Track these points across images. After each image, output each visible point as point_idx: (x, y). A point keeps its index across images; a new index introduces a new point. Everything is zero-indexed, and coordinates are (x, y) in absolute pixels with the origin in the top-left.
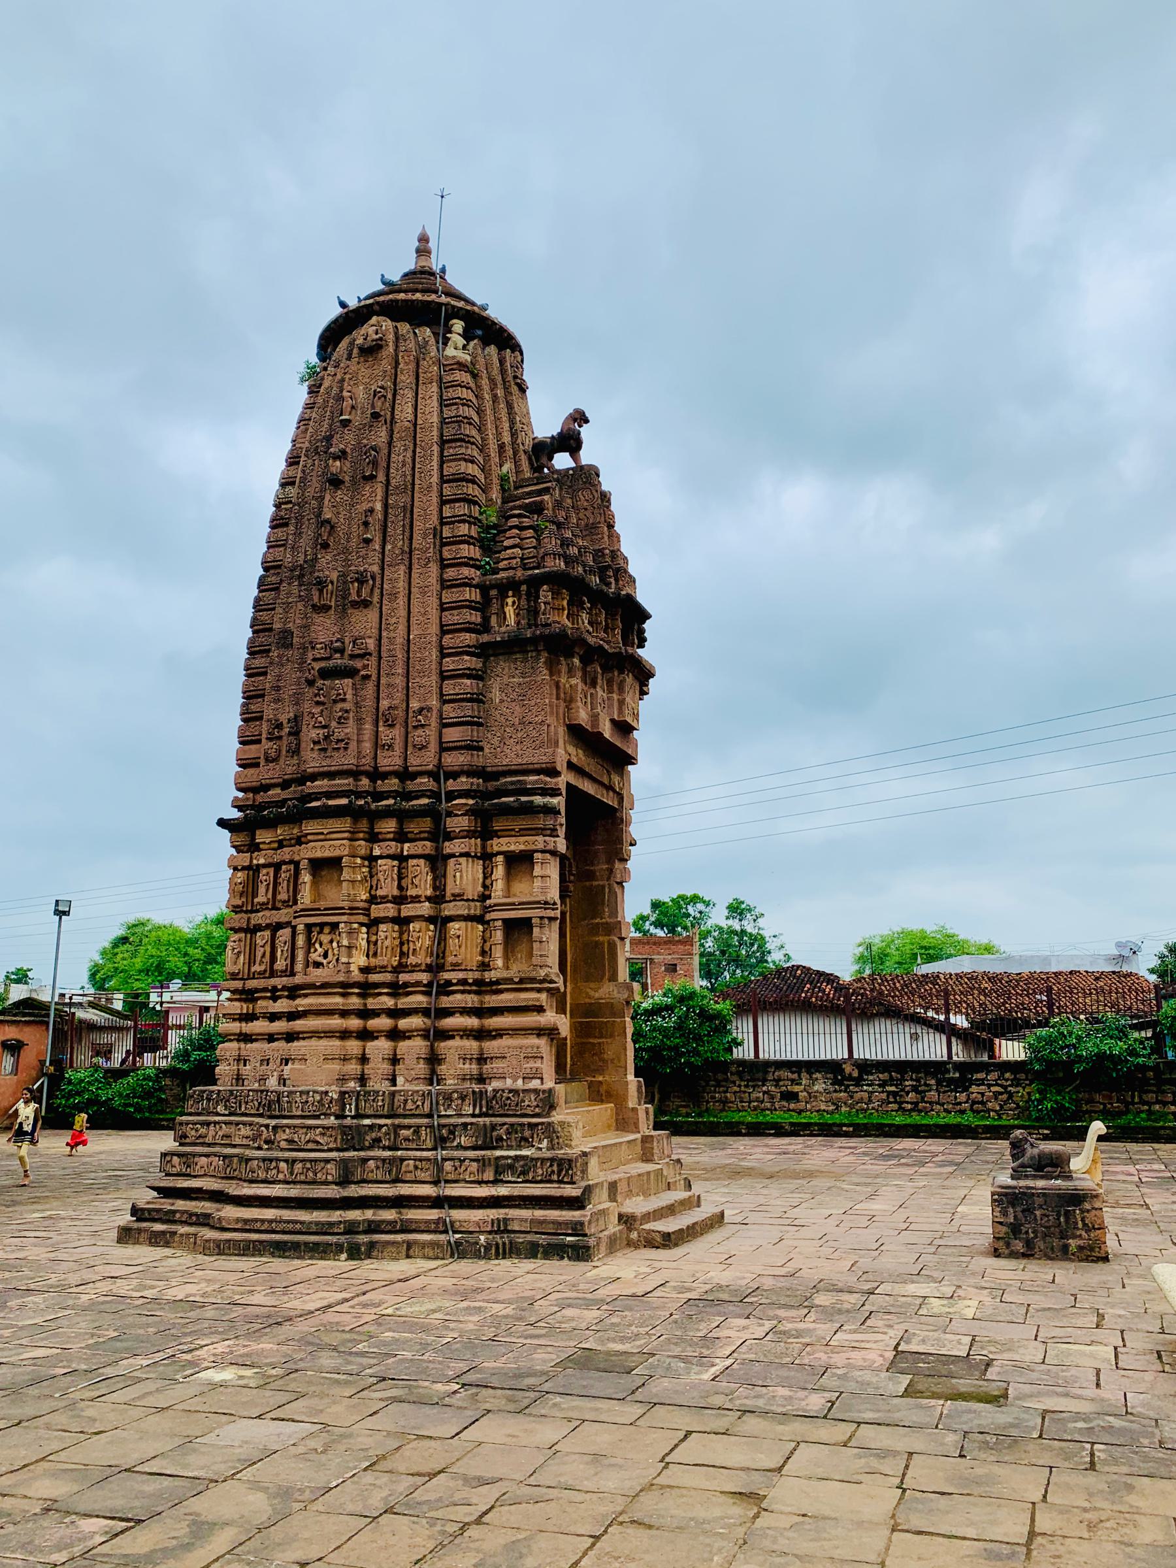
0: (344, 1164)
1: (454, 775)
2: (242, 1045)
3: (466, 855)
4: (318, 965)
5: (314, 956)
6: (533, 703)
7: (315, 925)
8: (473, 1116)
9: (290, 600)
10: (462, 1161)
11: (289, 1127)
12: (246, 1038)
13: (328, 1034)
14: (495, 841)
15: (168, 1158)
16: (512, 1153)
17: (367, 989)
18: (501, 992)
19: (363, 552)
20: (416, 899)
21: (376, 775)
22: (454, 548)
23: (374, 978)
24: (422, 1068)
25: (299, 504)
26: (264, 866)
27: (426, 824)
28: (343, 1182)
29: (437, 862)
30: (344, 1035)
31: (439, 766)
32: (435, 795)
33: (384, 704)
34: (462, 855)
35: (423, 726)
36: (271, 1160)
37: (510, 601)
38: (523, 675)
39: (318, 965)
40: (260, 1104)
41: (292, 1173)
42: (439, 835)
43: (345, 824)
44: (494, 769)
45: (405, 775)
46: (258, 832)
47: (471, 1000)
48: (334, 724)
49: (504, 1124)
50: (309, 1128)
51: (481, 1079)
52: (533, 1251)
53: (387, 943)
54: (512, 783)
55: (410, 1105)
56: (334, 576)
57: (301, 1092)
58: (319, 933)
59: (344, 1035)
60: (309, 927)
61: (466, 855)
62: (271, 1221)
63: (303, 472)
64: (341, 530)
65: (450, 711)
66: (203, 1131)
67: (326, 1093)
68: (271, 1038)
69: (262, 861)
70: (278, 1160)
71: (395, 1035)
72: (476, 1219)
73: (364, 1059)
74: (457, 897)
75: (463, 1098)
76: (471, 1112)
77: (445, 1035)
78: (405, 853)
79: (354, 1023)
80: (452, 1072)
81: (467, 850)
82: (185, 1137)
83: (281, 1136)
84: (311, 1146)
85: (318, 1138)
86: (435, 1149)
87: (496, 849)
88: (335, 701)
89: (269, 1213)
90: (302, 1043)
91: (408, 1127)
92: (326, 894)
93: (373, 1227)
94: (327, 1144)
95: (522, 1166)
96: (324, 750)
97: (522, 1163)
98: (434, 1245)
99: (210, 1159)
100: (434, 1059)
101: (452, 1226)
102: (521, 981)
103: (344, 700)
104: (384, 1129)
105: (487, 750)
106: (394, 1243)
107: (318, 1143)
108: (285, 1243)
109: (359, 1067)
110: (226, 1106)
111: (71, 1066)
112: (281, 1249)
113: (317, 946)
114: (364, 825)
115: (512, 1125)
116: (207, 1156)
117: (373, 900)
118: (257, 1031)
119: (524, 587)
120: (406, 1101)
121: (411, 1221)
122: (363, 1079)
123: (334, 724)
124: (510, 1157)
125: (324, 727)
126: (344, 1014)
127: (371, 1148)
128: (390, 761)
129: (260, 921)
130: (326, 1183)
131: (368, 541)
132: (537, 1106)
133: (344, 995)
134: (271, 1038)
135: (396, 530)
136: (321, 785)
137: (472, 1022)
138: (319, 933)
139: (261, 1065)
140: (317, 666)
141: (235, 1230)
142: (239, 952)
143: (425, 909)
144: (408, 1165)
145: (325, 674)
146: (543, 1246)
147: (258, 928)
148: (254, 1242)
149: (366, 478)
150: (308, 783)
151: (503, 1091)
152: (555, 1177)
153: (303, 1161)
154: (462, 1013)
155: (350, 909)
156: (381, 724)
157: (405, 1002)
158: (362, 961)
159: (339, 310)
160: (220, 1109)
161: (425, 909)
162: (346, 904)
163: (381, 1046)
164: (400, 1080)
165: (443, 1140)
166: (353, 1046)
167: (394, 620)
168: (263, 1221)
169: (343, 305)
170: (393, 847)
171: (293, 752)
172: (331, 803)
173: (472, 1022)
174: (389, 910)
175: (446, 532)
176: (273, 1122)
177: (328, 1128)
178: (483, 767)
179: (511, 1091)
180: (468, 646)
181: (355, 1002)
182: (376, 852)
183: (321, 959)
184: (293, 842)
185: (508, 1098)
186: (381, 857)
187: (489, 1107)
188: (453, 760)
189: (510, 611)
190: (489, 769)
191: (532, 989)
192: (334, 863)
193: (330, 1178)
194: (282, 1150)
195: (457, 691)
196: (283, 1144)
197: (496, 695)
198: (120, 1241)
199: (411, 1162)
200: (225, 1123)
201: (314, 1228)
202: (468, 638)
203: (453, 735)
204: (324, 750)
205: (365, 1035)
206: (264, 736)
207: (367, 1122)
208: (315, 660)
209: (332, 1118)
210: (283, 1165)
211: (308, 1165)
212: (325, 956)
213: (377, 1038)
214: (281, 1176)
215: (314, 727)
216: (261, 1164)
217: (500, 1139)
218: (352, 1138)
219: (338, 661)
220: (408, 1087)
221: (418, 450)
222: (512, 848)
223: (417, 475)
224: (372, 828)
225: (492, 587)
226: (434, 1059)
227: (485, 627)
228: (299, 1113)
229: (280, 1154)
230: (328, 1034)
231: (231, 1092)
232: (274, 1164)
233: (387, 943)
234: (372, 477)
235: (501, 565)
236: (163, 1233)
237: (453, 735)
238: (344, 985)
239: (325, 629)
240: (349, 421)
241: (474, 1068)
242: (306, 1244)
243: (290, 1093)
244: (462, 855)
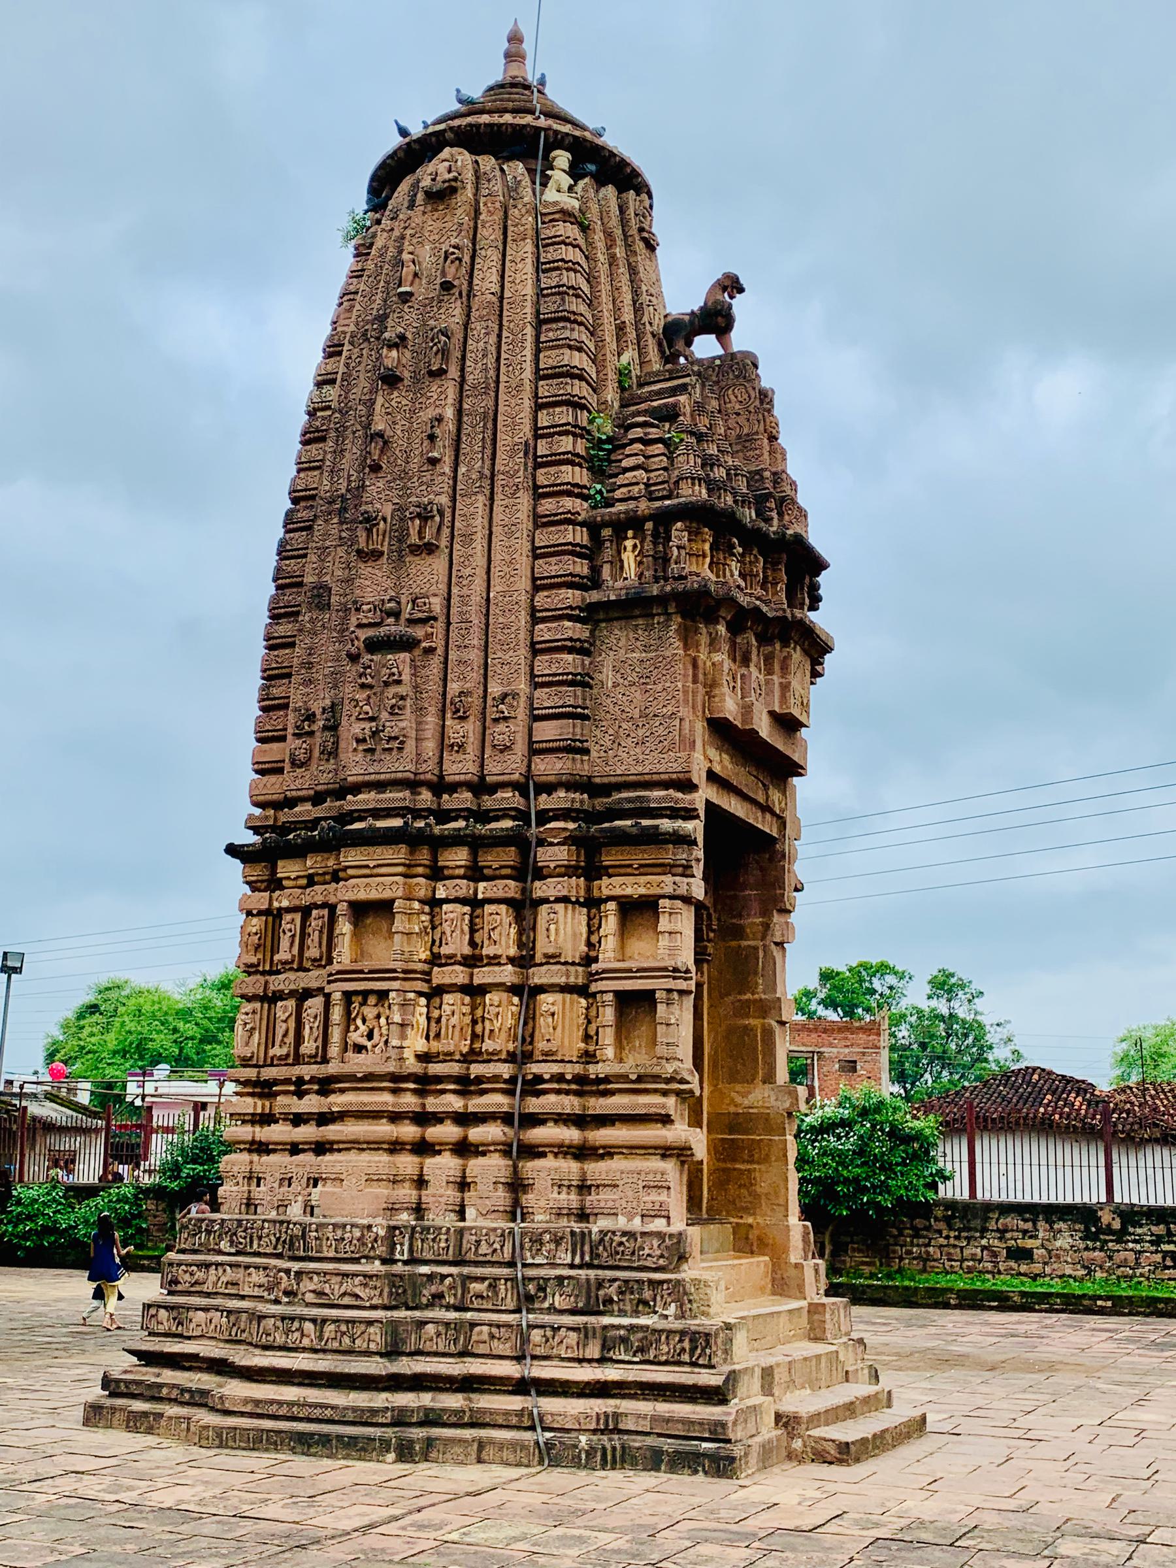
0: (393, 1327)
1: (548, 788)
2: (255, 1157)
3: (564, 900)
4: (359, 1049)
5: (355, 1037)
6: (659, 687)
7: (356, 993)
8: (572, 1266)
9: (328, 543)
10: (555, 1330)
11: (318, 1274)
12: (261, 1148)
13: (373, 1145)
14: (605, 881)
15: (153, 1311)
16: (626, 1321)
17: (426, 1084)
18: (612, 1093)
19: (427, 477)
20: (494, 960)
21: (440, 787)
22: (552, 470)
23: (435, 1069)
24: (501, 1197)
25: (340, 411)
26: (288, 910)
27: (509, 856)
28: (392, 1352)
29: (524, 909)
30: (395, 1147)
31: (528, 775)
32: (522, 816)
33: (454, 687)
34: (558, 900)
35: (506, 719)
36: (292, 1319)
37: (629, 544)
38: (646, 648)
39: (359, 1049)
40: (278, 1239)
41: (321, 1338)
42: (528, 871)
43: (397, 854)
44: (606, 780)
45: (481, 787)
46: (280, 863)
47: (570, 1104)
48: (384, 715)
49: (615, 1280)
50: (345, 1275)
51: (583, 1216)
52: (654, 1461)
53: (454, 1020)
54: (629, 800)
55: (484, 1249)
56: (387, 510)
57: (335, 1225)
58: (361, 1005)
59: (395, 1147)
60: (348, 996)
61: (564, 900)
62: (291, 1404)
63: (347, 365)
64: (399, 444)
65: (545, 699)
66: (200, 1275)
67: (370, 1227)
68: (294, 1149)
69: (285, 903)
70: (302, 1319)
71: (464, 1149)
72: (574, 1412)
73: (421, 1182)
74: (552, 959)
75: (557, 1241)
76: (569, 1261)
77: (532, 1151)
78: (480, 896)
79: (409, 1131)
80: (542, 1203)
81: (565, 893)
82: (177, 1282)
83: (307, 1285)
84: (347, 1300)
85: (357, 1291)
86: (518, 1311)
87: (606, 892)
88: (387, 684)
89: (290, 1393)
90: (336, 1157)
91: (482, 1279)
92: (371, 950)
93: (431, 1419)
95: (641, 1340)
96: (371, 751)
97: (640, 1335)
98: (514, 1445)
99: (210, 1315)
100: (517, 1186)
101: (541, 1421)
102: (640, 1079)
103: (399, 682)
104: (448, 1281)
105: (594, 754)
106: (461, 1441)
107: (357, 1296)
108: (312, 1435)
109: (414, 1192)
110: (232, 1242)
111: (21, 1180)
112: (304, 1443)
113: (359, 1022)
114: (424, 855)
115: (626, 1282)
116: (205, 1310)
117: (435, 960)
118: (276, 1137)
119: (649, 525)
120: (478, 1242)
121: (483, 1411)
122: (419, 1210)
123: (384, 715)
124: (623, 1327)
125: (372, 719)
126: (395, 1117)
127: (430, 1305)
128: (460, 767)
129: (281, 987)
130: (368, 1353)
131: (433, 462)
132: (662, 1256)
133: (395, 1091)
134: (294, 1149)
135: (472, 446)
136: (367, 799)
137: (571, 1135)
138: (361, 1005)
139: (281, 1185)
140: (363, 634)
141: (242, 1414)
142: (253, 1029)
143: (507, 974)
144: (481, 1333)
145: (373, 646)
146: (668, 1454)
147: (278, 996)
148: (268, 1431)
149: (432, 374)
150: (349, 797)
151: (614, 1233)
152: (686, 1358)
154: (556, 1122)
155: (405, 972)
156: (449, 715)
157: (477, 1104)
158: (421, 1045)
159: (397, 141)
160: (224, 1245)
161: (507, 974)
162: (398, 965)
163: (443, 1166)
164: (470, 1213)
165: (530, 1298)
166: (407, 1163)
167: (468, 571)
168: (280, 1403)
169: (403, 132)
170: (463, 888)
171: (330, 754)
172: (380, 824)
173: (571, 1135)
174: (457, 975)
175: (543, 448)
176: (296, 1266)
177: (371, 1277)
178: (589, 777)
179: (624, 1234)
180: (571, 608)
181: (409, 1102)
182: (441, 894)
183: (364, 1041)
184: (328, 877)
185: (621, 1244)
186: (447, 901)
187: (594, 1255)
188: (548, 767)
189: (629, 558)
190: (598, 780)
191: (656, 1091)
192: (384, 908)
193: (373, 1346)
194: (308, 1305)
195: (554, 670)
196: (310, 1297)
197: (607, 676)
198: (87, 1422)
199: (485, 1329)
200: (231, 1266)
201: (350, 1416)
202: (571, 597)
203: (547, 731)
204: (371, 751)
205: (423, 1148)
206: (290, 730)
207: (425, 1270)
208: (360, 626)
209: (377, 1263)
210: (308, 1327)
211: (343, 1328)
212: (370, 1036)
213: (439, 1152)
214: (306, 1342)
215: (358, 719)
216: (279, 1324)
217: (609, 1301)
218: (403, 1293)
219: (391, 628)
220: (482, 1223)
221: (505, 334)
222: (629, 891)
223: (503, 369)
224: (435, 860)
225: (605, 524)
226: (517, 1186)
227: (594, 581)
228: (332, 1254)
229: (306, 1311)
230: (373, 1145)
231: (239, 1221)
232: (296, 1324)
233: (454, 1020)
234: (441, 373)
235: (618, 494)
236: (145, 1414)
237: (547, 731)
238: (395, 1078)
239: (374, 583)
240: (411, 294)
241: (572, 1199)
242: (339, 1437)
243: (320, 1226)
244: (558, 900)
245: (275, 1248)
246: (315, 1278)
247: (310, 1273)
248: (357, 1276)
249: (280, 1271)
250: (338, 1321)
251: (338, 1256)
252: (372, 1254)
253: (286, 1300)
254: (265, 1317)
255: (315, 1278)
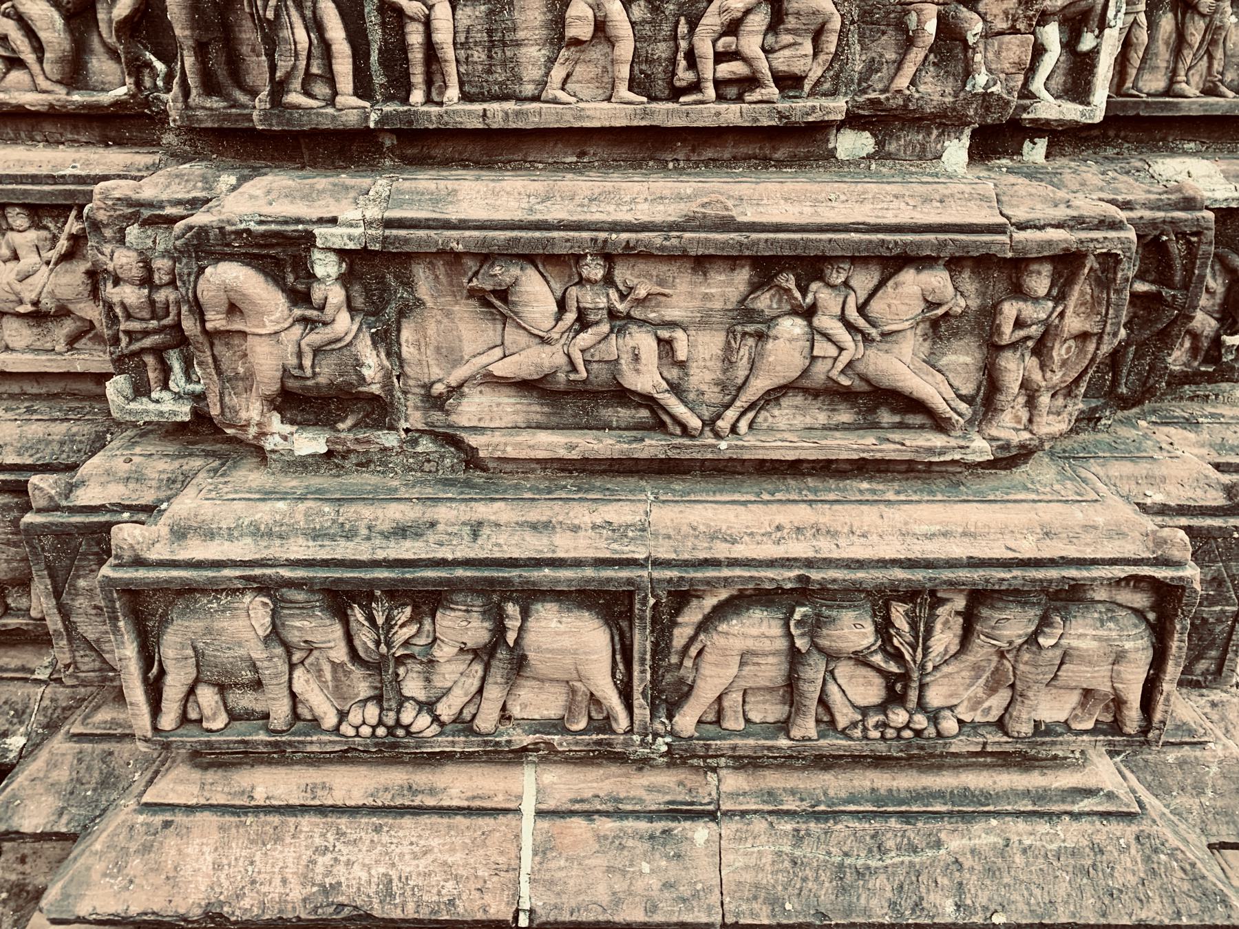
50: (784, 266)
70: (505, 591)
83: (446, 338)
84: (790, 431)
85: (902, 366)
94: (987, 398)
153: (801, 596)
176: (345, 208)
194: (471, 467)
210: (570, 641)
229: (506, 529)
245: (75, 72)
246: (536, 294)
247: (483, 268)
248: (893, 263)
249: (207, 247)
250: (804, 592)
251: (666, 114)
252: (934, 91)
253: (310, 443)
254: (187, 591)
255: (536, 294)
